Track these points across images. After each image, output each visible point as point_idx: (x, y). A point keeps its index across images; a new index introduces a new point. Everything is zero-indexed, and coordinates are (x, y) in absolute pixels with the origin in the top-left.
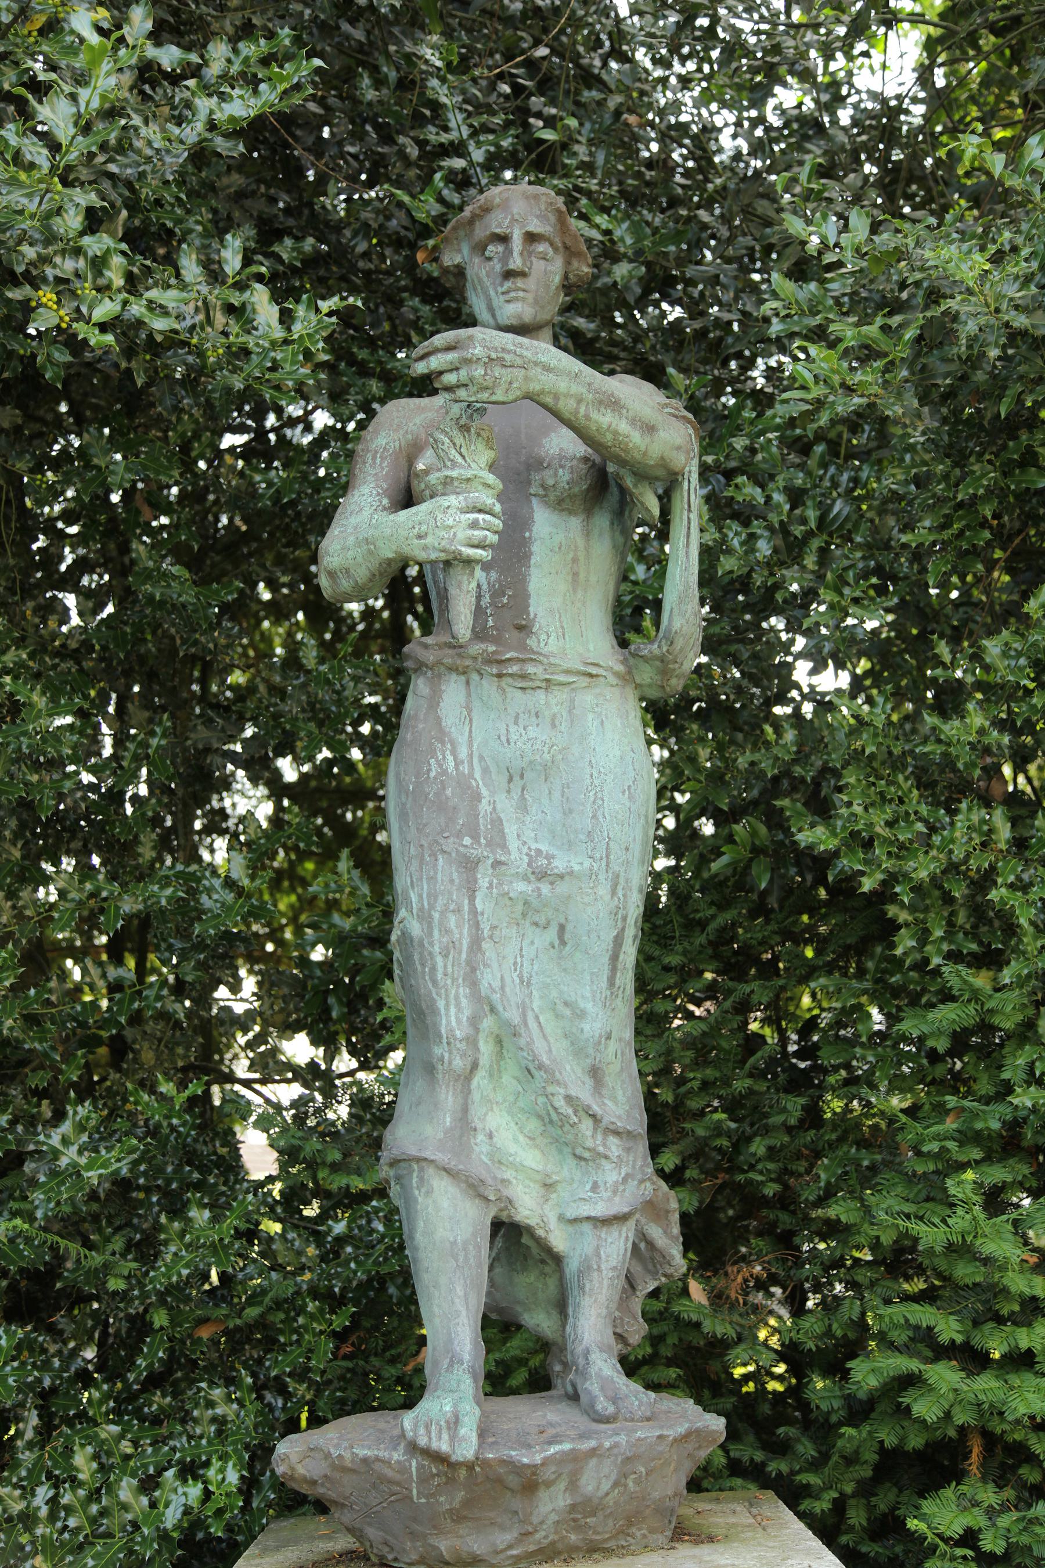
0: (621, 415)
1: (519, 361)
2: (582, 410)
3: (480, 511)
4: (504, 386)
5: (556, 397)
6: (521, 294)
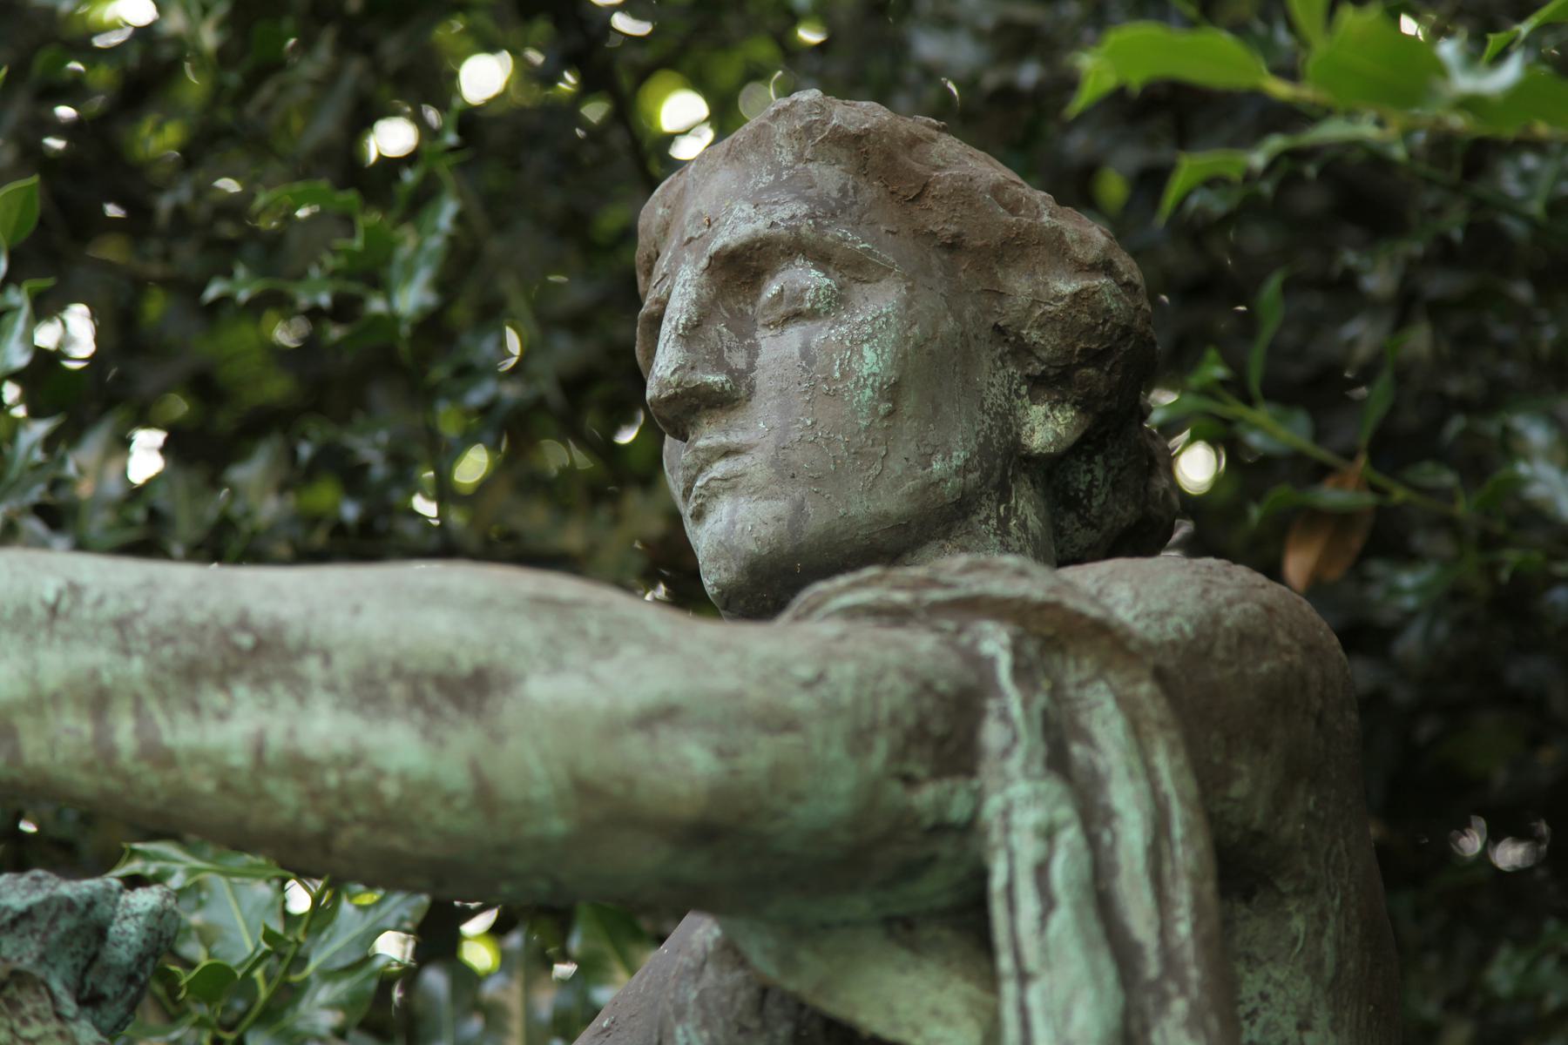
0: (300, 688)
2: (124, 733)
6: (719, 468)
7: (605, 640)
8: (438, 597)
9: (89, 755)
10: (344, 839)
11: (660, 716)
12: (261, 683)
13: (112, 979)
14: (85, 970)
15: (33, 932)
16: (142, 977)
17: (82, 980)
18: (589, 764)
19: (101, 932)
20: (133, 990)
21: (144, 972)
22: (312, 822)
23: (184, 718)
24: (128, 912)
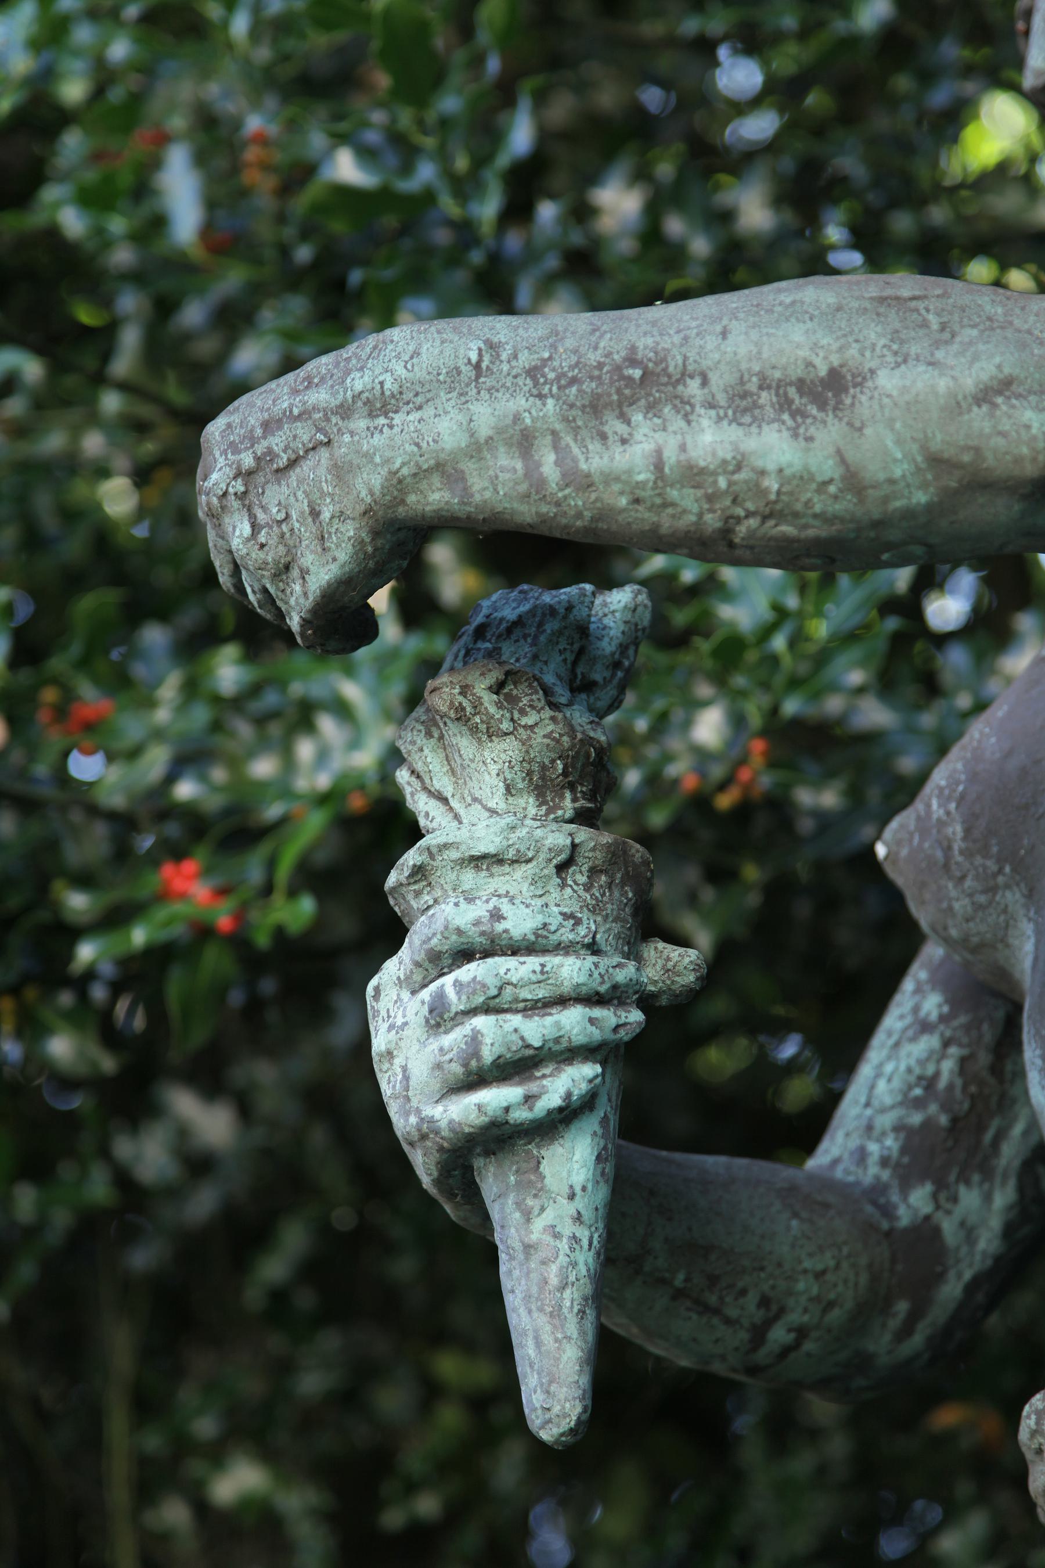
0: (685, 408)
1: (304, 433)
3: (465, 955)
4: (307, 532)
5: (444, 469)
7: (943, 327)
8: (794, 312)
9: (523, 488)
10: (742, 530)
11: (997, 390)
12: (652, 408)
13: (599, 667)
14: (575, 663)
15: (525, 637)
16: (627, 663)
17: (573, 671)
18: (938, 441)
19: (583, 630)
20: (620, 674)
21: (628, 658)
22: (712, 521)
23: (595, 446)
24: (606, 610)
